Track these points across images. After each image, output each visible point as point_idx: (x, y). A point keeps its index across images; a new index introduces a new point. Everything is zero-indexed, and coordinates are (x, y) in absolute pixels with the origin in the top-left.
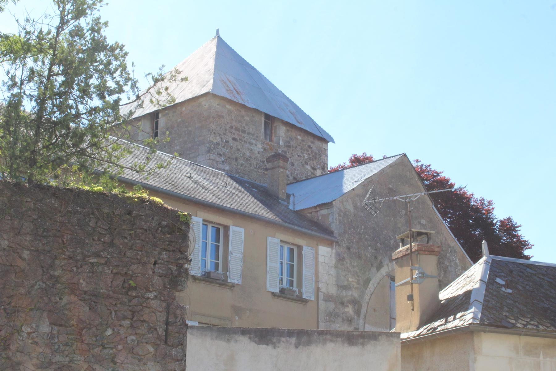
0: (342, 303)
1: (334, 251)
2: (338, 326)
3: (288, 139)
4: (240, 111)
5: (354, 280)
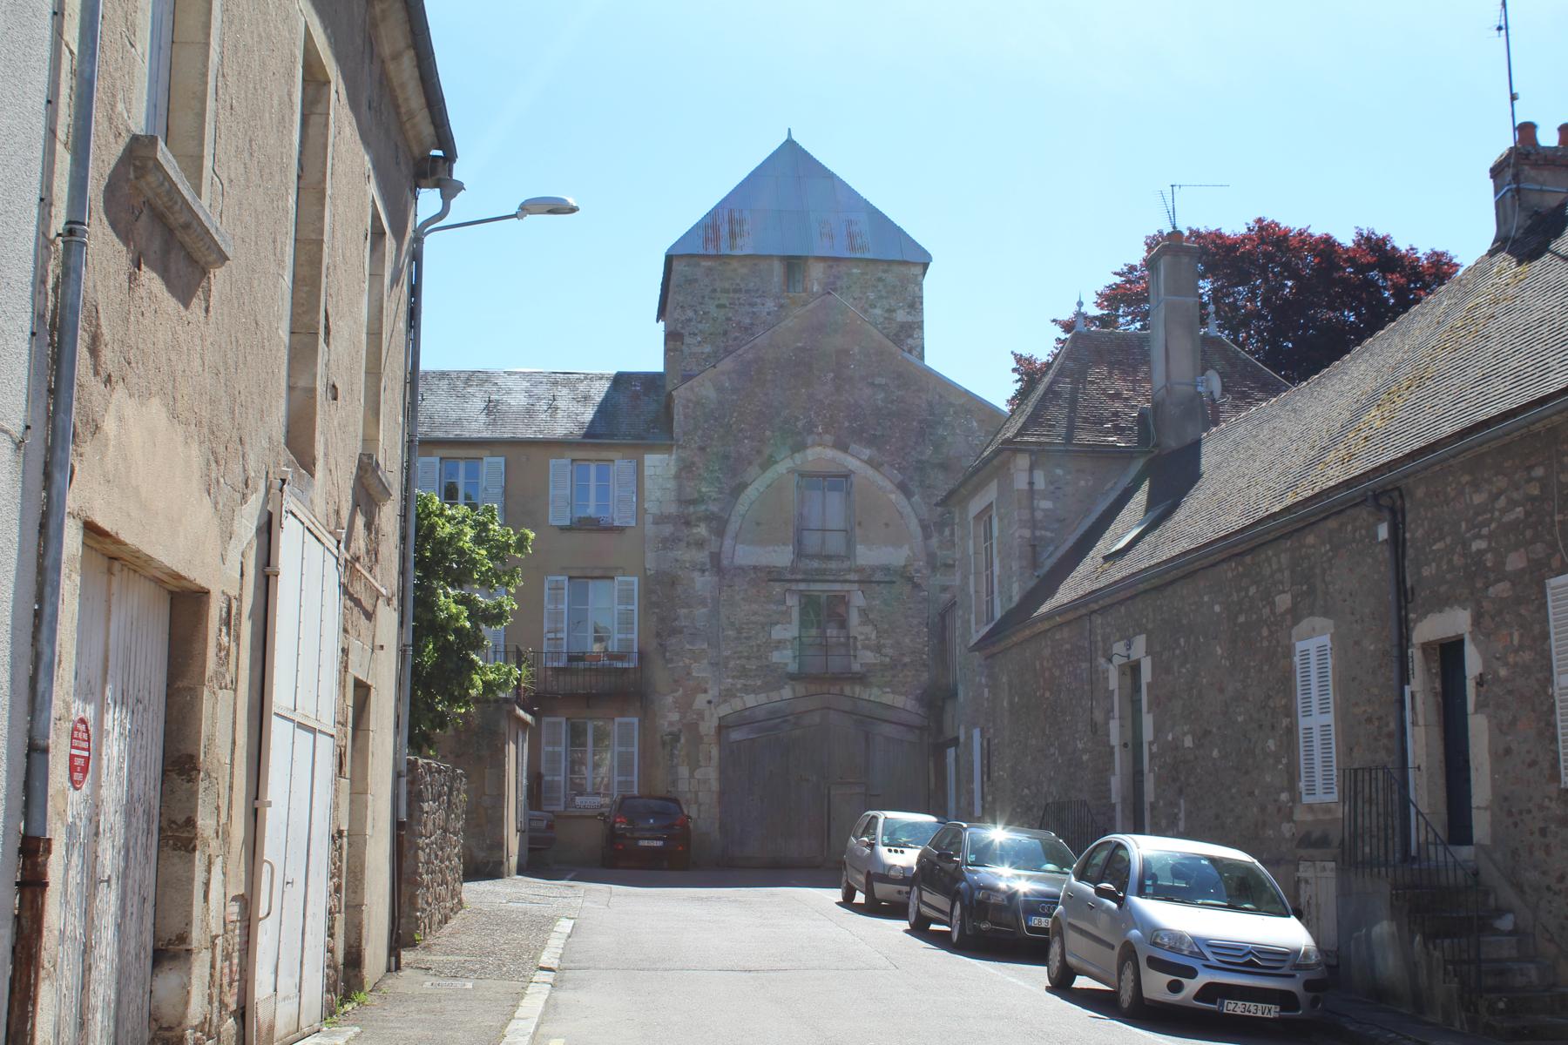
1: (674, 457)
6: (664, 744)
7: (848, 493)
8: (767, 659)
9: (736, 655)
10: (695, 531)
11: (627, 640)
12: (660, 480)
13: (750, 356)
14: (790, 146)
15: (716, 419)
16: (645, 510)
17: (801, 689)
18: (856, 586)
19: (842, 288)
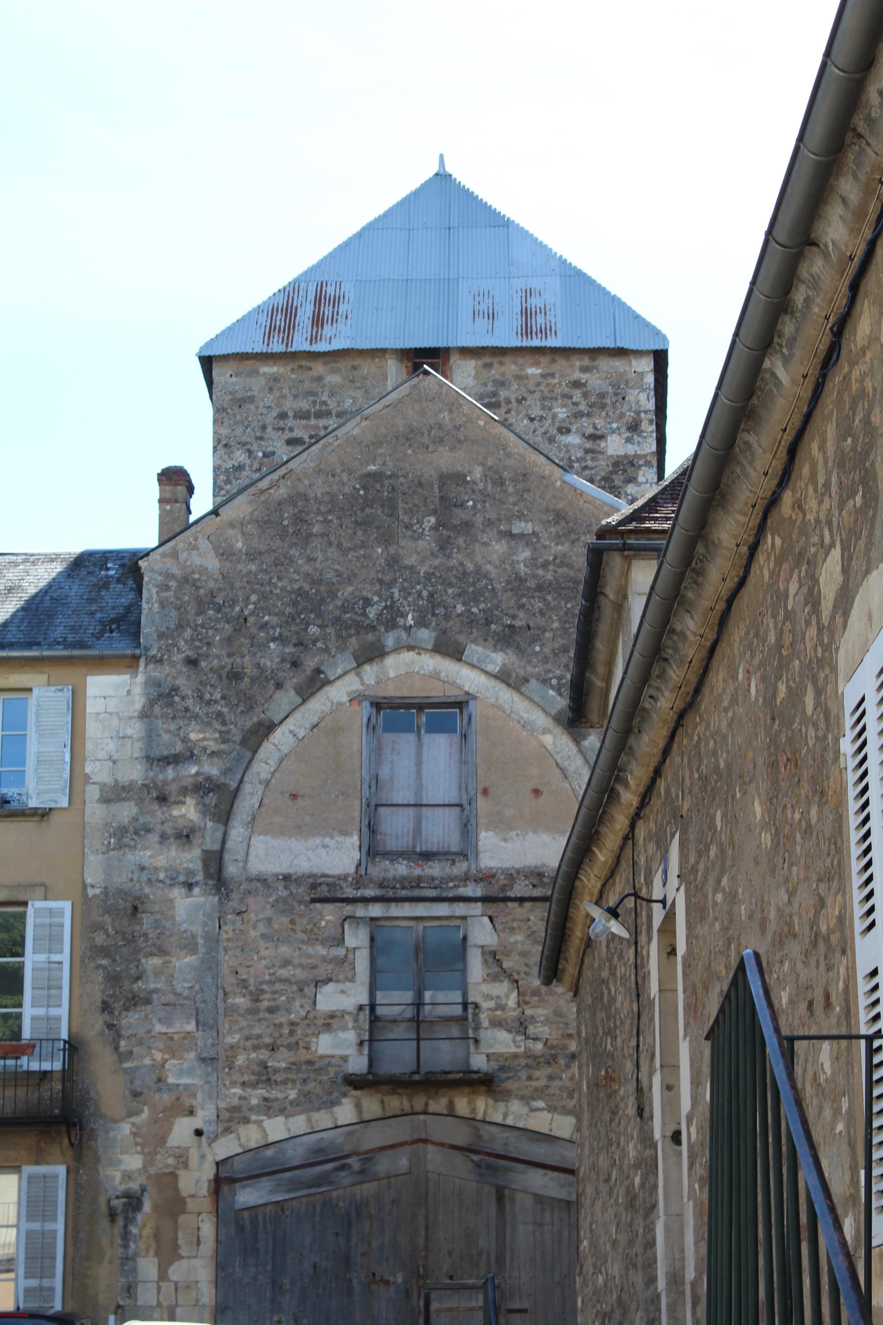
0: (162, 799)
1: (140, 678)
2: (149, 854)
3: (490, 388)
4: (310, 369)
5: (208, 735)
6: (112, 1215)
7: (465, 736)
8: (307, 1048)
9: (249, 1044)
10: (175, 813)
11: (48, 1018)
12: (116, 721)
13: (282, 492)
14: (442, 178)
15: (219, 609)
16: (87, 778)
17: (372, 1105)
18: (477, 909)
19: (508, 402)
